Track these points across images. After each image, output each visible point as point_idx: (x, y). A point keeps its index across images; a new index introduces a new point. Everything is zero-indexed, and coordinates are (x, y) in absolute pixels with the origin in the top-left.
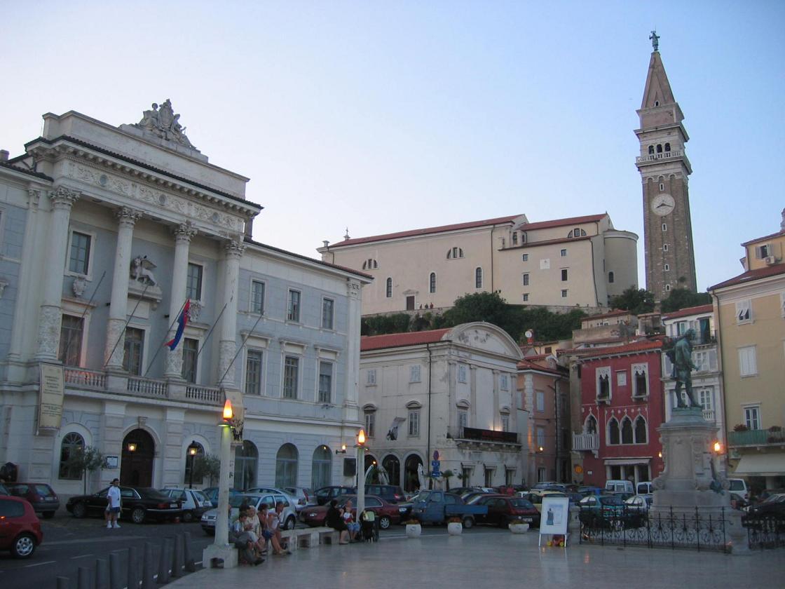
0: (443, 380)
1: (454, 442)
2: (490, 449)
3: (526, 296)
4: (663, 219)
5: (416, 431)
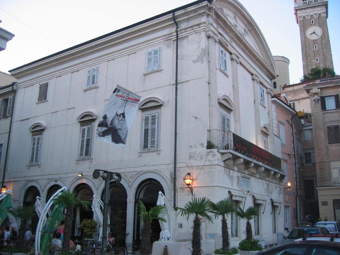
0: (199, 59)
1: (219, 155)
2: (258, 176)
4: (314, 42)
5: (153, 142)
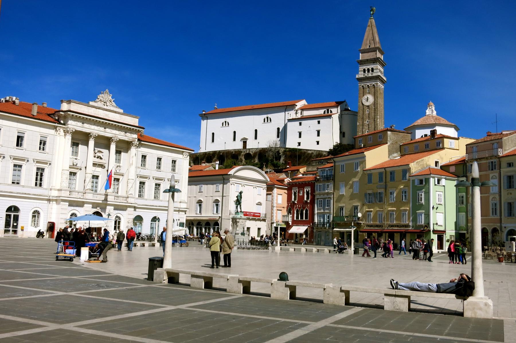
3: (299, 144)
4: (368, 106)
